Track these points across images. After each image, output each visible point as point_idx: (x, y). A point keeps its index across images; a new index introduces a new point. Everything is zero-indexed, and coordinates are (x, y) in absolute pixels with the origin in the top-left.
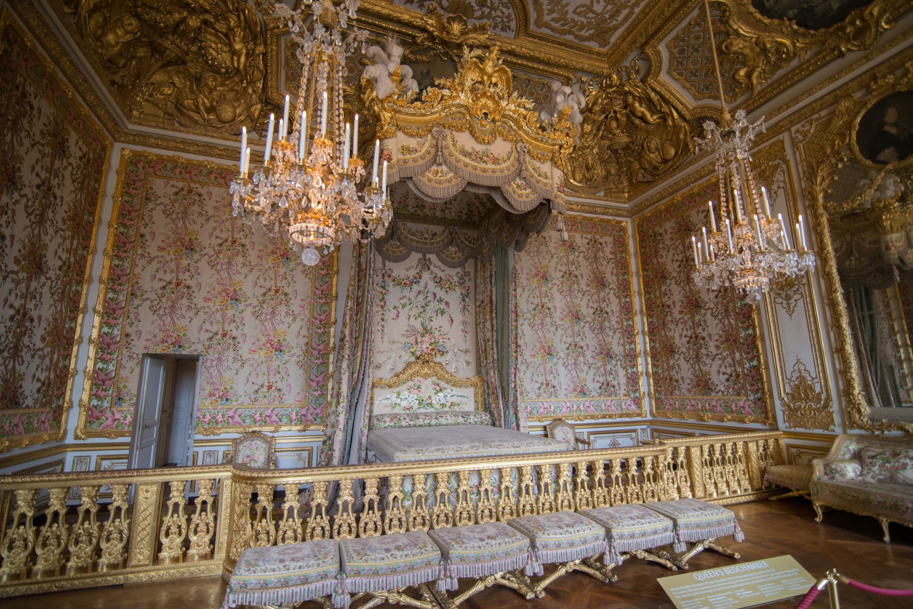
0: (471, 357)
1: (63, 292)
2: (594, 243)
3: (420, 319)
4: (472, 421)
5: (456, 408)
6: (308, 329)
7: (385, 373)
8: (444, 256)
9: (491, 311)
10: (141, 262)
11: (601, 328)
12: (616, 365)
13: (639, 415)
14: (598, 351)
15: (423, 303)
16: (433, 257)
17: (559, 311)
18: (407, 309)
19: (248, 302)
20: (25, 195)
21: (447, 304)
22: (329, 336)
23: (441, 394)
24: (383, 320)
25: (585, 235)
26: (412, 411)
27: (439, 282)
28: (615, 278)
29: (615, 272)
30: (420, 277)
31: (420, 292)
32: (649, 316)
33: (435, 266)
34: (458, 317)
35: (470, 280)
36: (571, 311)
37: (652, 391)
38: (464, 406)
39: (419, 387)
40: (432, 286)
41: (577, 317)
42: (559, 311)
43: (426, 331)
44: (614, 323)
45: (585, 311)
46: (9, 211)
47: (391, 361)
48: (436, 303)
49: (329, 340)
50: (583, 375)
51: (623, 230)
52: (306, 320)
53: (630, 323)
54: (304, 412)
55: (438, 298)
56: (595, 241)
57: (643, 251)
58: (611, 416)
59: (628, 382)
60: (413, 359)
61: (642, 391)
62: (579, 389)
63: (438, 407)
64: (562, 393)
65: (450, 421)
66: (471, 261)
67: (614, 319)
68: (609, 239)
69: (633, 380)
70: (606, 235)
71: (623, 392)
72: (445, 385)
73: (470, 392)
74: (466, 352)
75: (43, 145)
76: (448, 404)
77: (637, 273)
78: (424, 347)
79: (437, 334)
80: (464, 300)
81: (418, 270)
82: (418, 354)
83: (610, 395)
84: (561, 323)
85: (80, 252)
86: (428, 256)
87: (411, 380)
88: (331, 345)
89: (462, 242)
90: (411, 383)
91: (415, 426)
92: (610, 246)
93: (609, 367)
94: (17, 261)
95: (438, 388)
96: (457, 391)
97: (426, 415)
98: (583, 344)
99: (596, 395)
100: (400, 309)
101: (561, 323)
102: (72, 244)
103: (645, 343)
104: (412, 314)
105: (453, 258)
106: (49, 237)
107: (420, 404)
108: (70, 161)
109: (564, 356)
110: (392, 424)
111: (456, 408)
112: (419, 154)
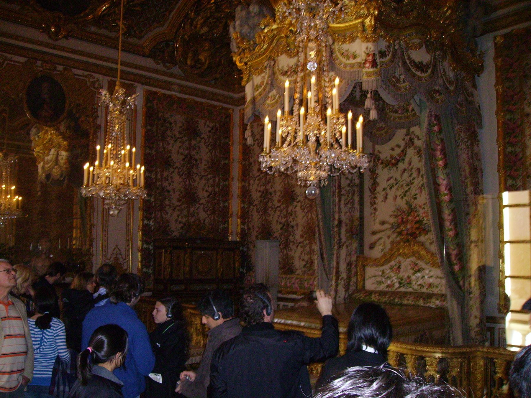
1: (214, 209)
3: (405, 198)
7: (376, 253)
10: (252, 182)
15: (408, 180)
18: (394, 189)
19: (298, 200)
20: (177, 167)
23: (419, 274)
24: (375, 203)
33: (419, 139)
39: (399, 267)
43: (411, 209)
46: (169, 178)
47: (381, 241)
48: (420, 178)
75: (181, 138)
85: (222, 184)
86: (412, 129)
90: (393, 263)
94: (179, 200)
102: (214, 181)
106: (197, 182)
107: (400, 283)
108: (202, 136)
111: (435, 290)
112: (263, 87)
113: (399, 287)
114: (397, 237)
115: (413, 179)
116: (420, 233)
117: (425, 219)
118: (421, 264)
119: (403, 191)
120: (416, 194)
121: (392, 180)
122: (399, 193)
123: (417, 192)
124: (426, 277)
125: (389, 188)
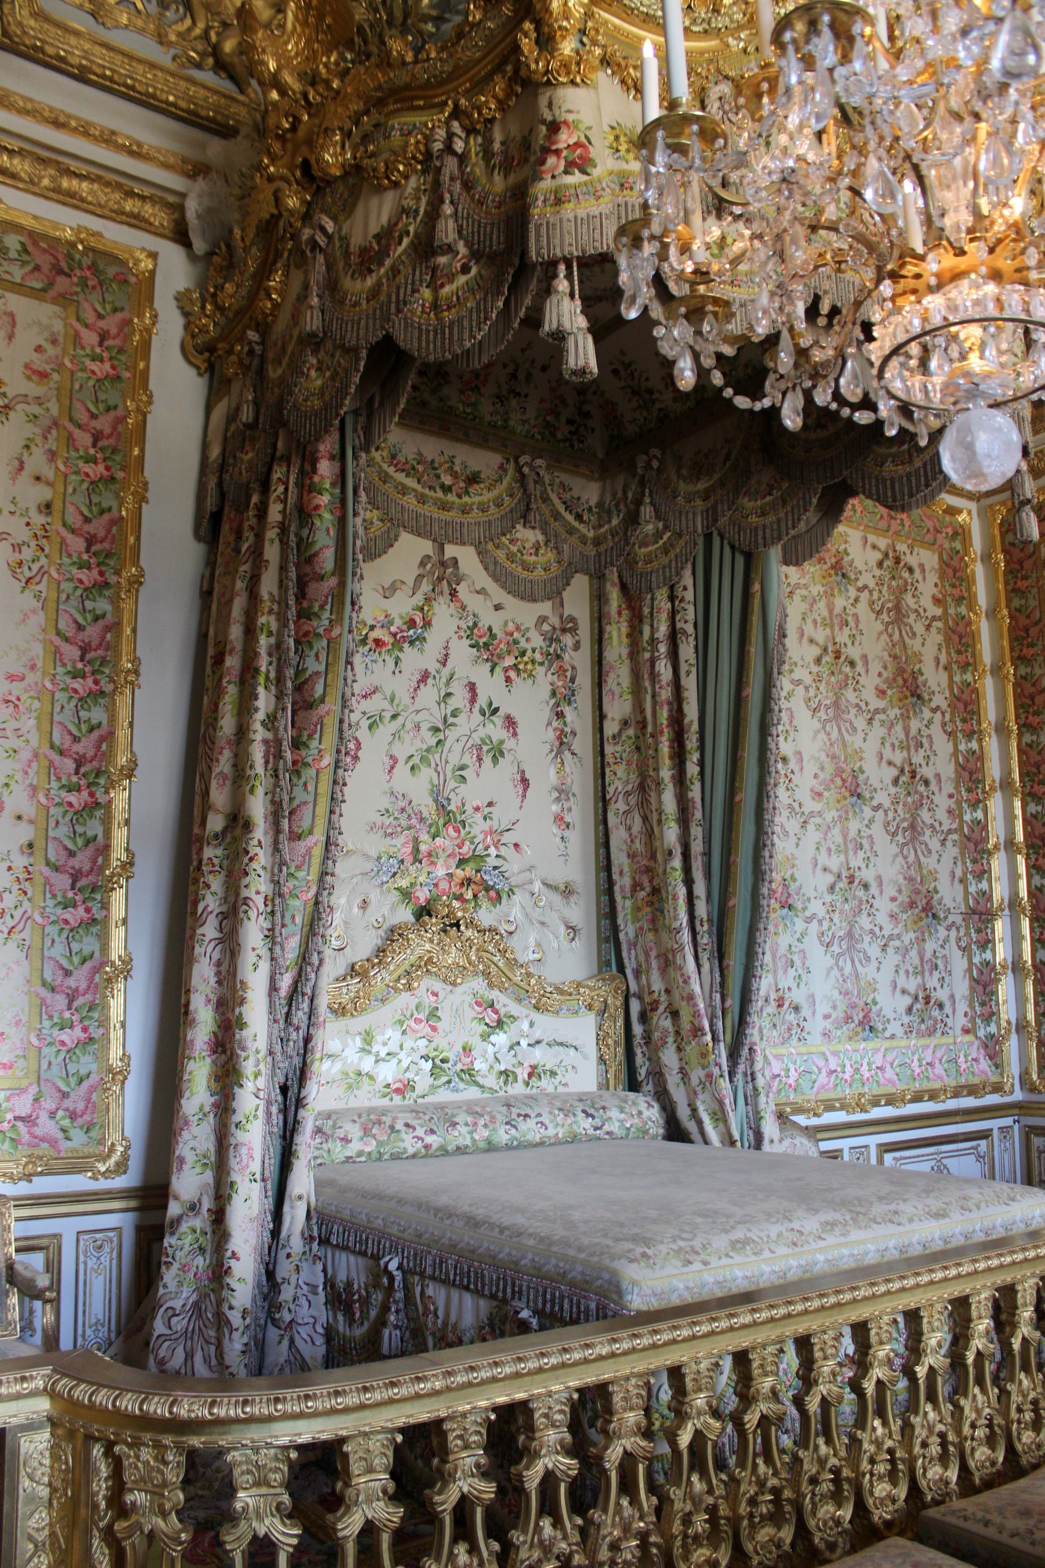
0: (581, 911)
2: (893, 562)
3: (427, 774)
4: (614, 1127)
5: (546, 1084)
6: (34, 789)
8: (501, 555)
9: (679, 756)
11: (913, 827)
12: (946, 940)
13: (997, 1088)
14: (903, 898)
16: (466, 557)
17: (810, 768)
21: (510, 723)
22: (107, 822)
23: (500, 1039)
25: (872, 538)
26: (411, 1097)
27: (486, 646)
28: (944, 676)
29: (943, 658)
30: (427, 624)
31: (425, 677)
32: (1029, 797)
34: (545, 775)
35: (577, 646)
36: (839, 772)
37: (1031, 1016)
38: (570, 1077)
40: (462, 652)
41: (854, 790)
42: (810, 768)
43: (448, 816)
44: (941, 814)
45: (878, 776)
49: (108, 834)
50: (868, 972)
51: (961, 533)
52: (26, 755)
53: (979, 815)
54: (23, 1106)
55: (482, 701)
56: (898, 560)
57: (1016, 603)
58: (933, 1096)
59: (972, 990)
60: (405, 915)
61: (1004, 1016)
62: (858, 1016)
63: (491, 1081)
64: (816, 1025)
65: (551, 1132)
66: (580, 584)
67: (942, 802)
68: (926, 558)
69: (984, 983)
70: (923, 544)
71: (961, 1021)
72: (514, 1008)
73: (583, 1029)
74: (567, 891)
76: (523, 1074)
77: (997, 670)
78: (440, 872)
79: (478, 827)
80: (560, 715)
81: (418, 599)
82: (422, 895)
83: (931, 1032)
84: (816, 806)
86: (451, 551)
87: (409, 987)
88: (118, 853)
89: (557, 516)
90: (404, 1001)
91: (444, 1152)
92: (933, 578)
93: (930, 946)
95: (491, 1017)
96: (547, 1026)
97: (473, 1110)
98: (867, 875)
99: (900, 1032)
100: (363, 734)
101: (816, 806)
103: (1014, 877)
104: (401, 751)
105: (527, 567)
109: (821, 912)
110: (371, 1146)
113: (434, 1088)
114: (393, 908)
115: (454, 714)
116: (475, 896)
117: (493, 851)
118: (506, 1003)
119: (418, 744)
120: (462, 768)
121: (377, 697)
122: (401, 751)
123: (467, 759)
124: (524, 1043)
125: (365, 723)
